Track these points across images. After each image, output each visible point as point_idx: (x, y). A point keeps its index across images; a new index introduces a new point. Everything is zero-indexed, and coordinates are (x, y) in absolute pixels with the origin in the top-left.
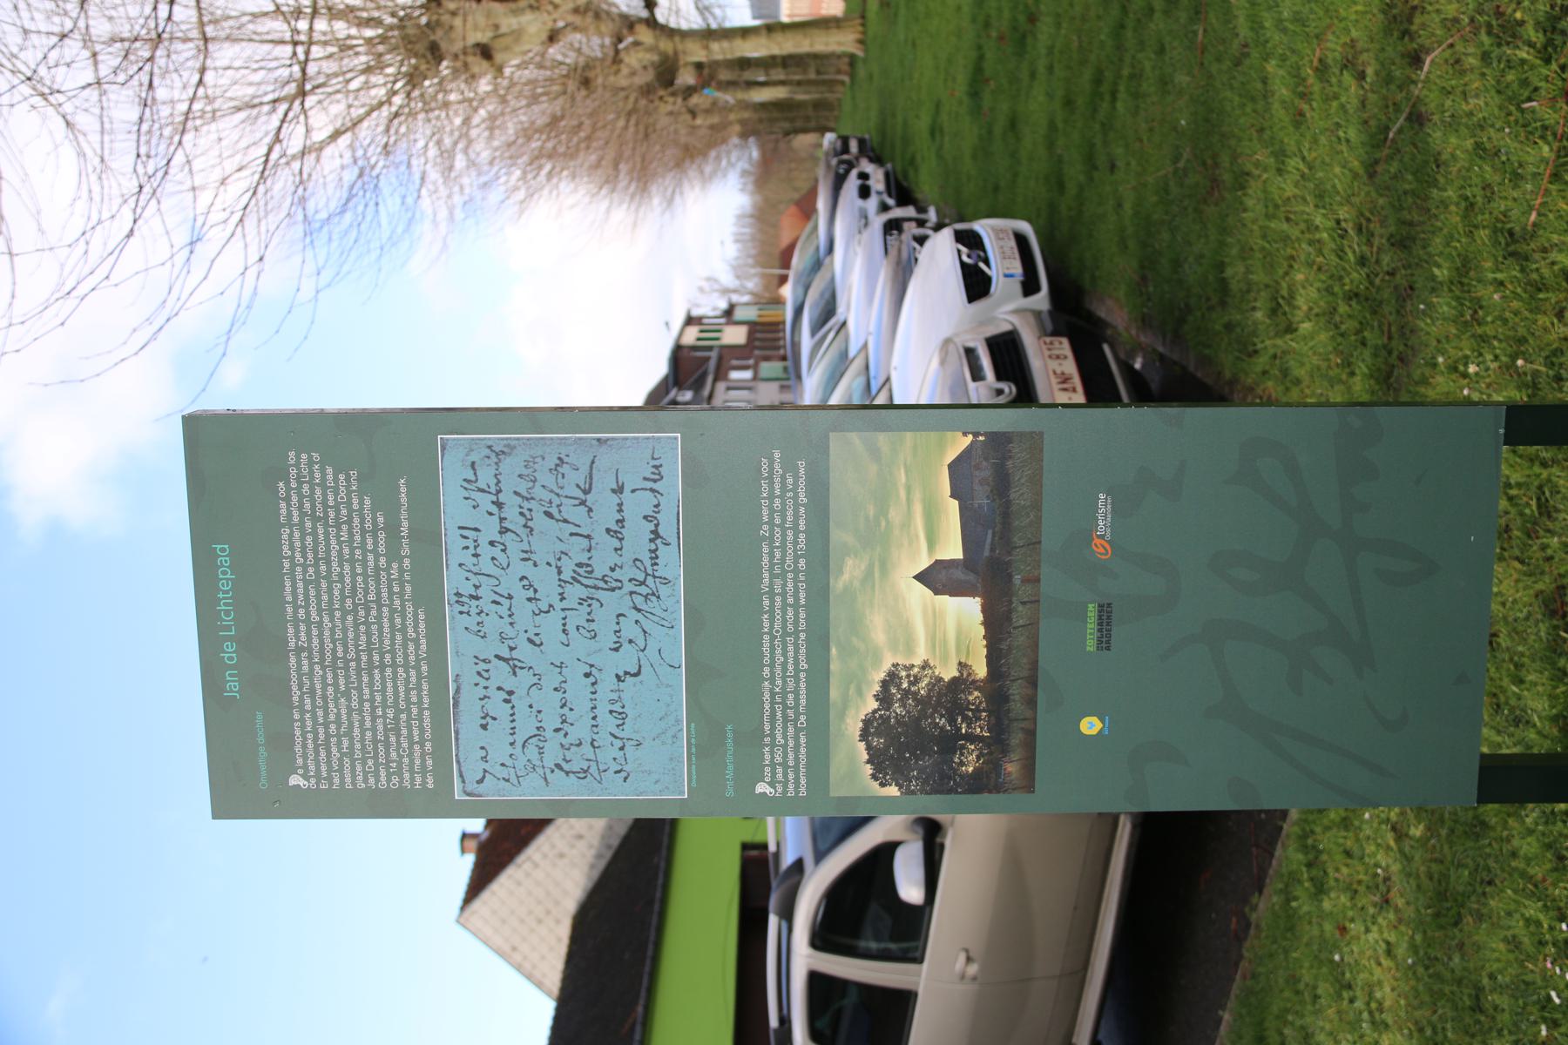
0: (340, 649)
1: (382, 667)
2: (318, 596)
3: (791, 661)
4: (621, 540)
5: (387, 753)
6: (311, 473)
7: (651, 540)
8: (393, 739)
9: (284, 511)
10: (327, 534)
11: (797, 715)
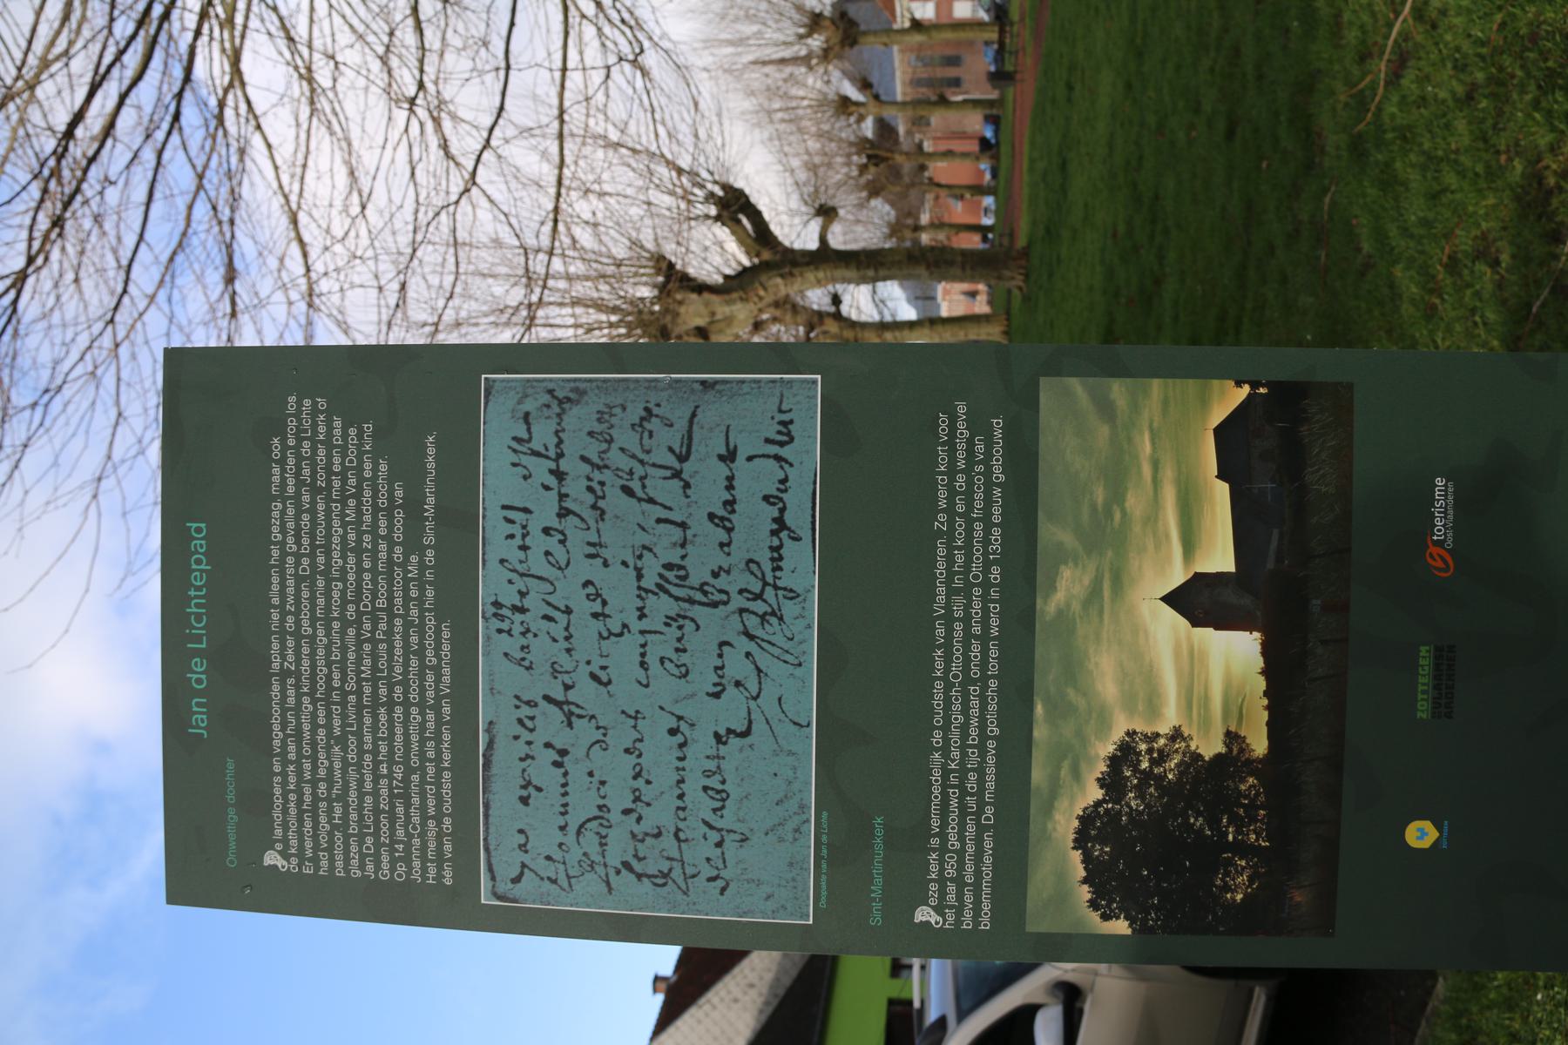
0: (336, 676)
1: (390, 705)
2: (313, 599)
3: (974, 722)
4: (730, 530)
5: (392, 829)
6: (315, 425)
7: (774, 533)
8: (400, 810)
9: (276, 479)
10: (328, 511)
11: (981, 805)
